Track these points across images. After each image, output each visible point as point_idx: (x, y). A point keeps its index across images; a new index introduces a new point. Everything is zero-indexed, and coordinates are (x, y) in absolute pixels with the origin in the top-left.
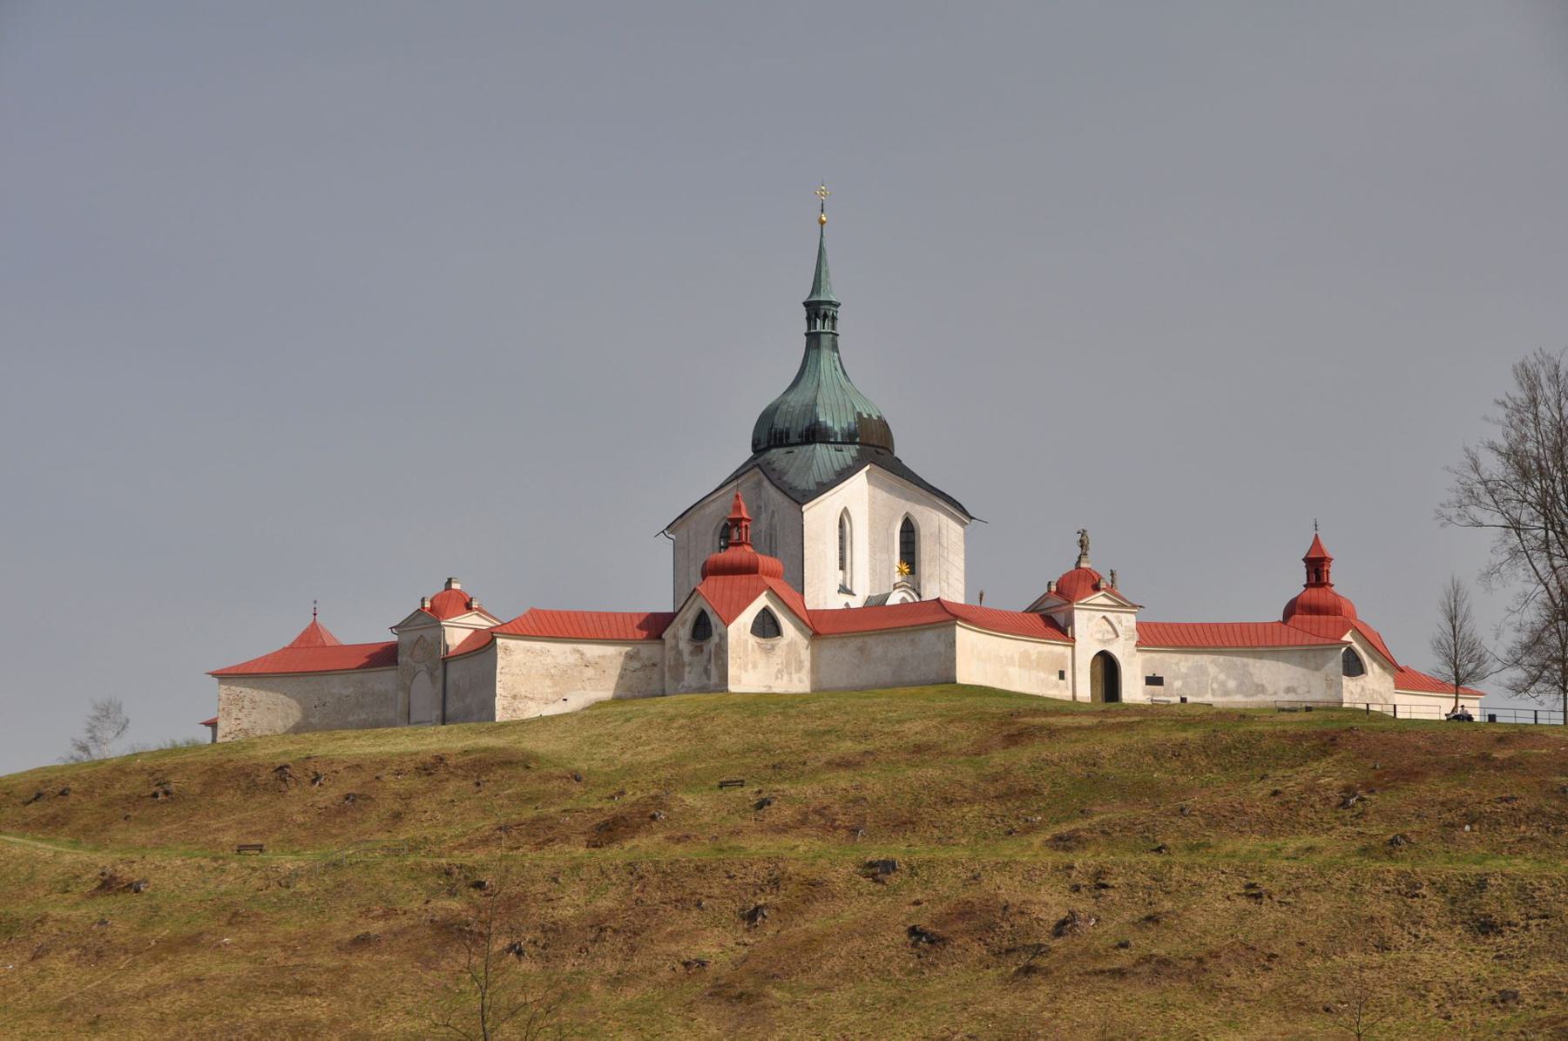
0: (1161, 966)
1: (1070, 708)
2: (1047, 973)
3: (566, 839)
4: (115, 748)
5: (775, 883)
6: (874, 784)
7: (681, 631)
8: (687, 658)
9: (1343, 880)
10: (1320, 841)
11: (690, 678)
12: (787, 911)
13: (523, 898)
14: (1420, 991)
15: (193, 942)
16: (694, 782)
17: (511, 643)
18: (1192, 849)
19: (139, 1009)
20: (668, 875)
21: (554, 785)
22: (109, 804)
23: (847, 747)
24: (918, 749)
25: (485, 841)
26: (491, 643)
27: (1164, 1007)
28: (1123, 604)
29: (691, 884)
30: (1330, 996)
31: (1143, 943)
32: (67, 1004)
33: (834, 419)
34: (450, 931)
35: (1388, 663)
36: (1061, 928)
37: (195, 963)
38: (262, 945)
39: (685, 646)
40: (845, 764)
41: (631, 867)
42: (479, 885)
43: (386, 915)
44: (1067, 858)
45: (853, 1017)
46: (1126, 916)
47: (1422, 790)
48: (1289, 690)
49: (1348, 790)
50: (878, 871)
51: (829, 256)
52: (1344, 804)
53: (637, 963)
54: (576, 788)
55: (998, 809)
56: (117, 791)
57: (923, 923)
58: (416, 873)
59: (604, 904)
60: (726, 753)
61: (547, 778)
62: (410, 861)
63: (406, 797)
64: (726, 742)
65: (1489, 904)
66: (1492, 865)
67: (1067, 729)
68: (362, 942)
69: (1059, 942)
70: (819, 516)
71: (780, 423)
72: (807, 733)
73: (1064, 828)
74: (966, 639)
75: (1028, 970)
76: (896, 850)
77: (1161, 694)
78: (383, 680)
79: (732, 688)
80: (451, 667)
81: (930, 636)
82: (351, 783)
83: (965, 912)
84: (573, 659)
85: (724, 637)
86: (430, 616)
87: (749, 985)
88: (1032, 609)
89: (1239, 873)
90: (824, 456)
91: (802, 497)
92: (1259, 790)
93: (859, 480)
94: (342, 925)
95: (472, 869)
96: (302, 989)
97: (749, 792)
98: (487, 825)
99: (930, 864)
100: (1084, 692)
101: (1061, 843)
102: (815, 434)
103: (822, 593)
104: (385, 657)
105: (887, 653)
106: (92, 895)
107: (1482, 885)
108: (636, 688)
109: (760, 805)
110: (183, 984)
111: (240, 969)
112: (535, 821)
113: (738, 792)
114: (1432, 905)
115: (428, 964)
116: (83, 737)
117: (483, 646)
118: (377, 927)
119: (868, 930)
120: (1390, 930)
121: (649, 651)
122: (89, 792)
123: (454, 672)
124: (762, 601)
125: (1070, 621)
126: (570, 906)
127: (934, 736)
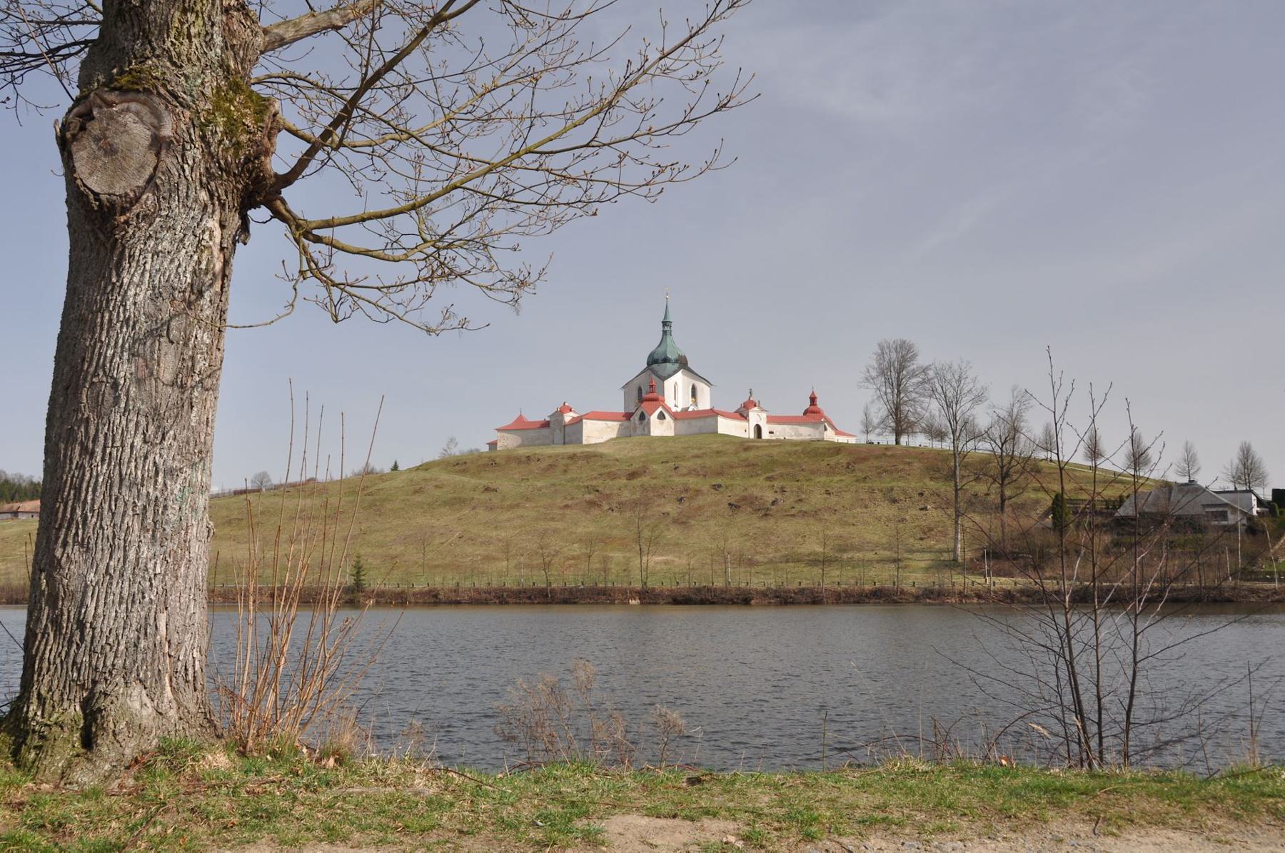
0: (804, 514)
1: (748, 440)
2: (771, 515)
3: (620, 478)
4: (456, 451)
5: (686, 491)
6: (708, 462)
7: (636, 418)
8: (638, 426)
9: (853, 488)
10: (843, 478)
11: (638, 432)
12: (691, 498)
13: (611, 494)
15: (517, 506)
17: (588, 421)
18: (807, 480)
19: (508, 524)
20: (654, 488)
21: (611, 463)
22: (479, 466)
23: (696, 452)
24: (718, 452)
25: (596, 478)
26: (581, 420)
27: (808, 525)
28: (762, 410)
29: (661, 491)
30: (853, 521)
31: (798, 507)
33: (671, 356)
34: (592, 504)
35: (833, 428)
36: (774, 503)
37: (520, 512)
38: (536, 507)
39: (637, 422)
40: (697, 456)
41: (642, 486)
42: (598, 491)
43: (572, 498)
44: (772, 483)
45: (717, 528)
46: (792, 499)
48: (809, 435)
49: (848, 464)
50: (716, 487)
51: (669, 309)
52: (848, 467)
53: (649, 513)
54: (617, 463)
56: (480, 463)
57: (732, 502)
58: (578, 487)
59: (635, 497)
60: (660, 453)
61: (609, 460)
63: (567, 465)
64: (659, 450)
65: (895, 495)
67: (761, 447)
68: (567, 506)
69: (772, 507)
70: (669, 384)
71: (656, 357)
72: (684, 448)
74: (720, 419)
75: (766, 515)
76: (718, 481)
77: (773, 437)
78: (545, 431)
79: (652, 434)
80: (567, 428)
81: (709, 420)
82: (550, 461)
83: (744, 498)
84: (605, 426)
85: (649, 420)
86: (560, 412)
87: (684, 519)
88: (736, 412)
89: (823, 487)
91: (664, 379)
93: (680, 373)
94: (560, 501)
95: (594, 486)
96: (553, 519)
97: (671, 464)
98: (595, 474)
99: (732, 485)
100: (752, 435)
101: (769, 479)
102: (666, 360)
104: (546, 425)
105: (697, 424)
106: (483, 492)
107: (892, 489)
108: (624, 434)
109: (676, 468)
110: (518, 517)
111: (533, 514)
112: (609, 473)
113: (668, 465)
114: (879, 495)
115: (587, 513)
117: (578, 422)
118: (570, 502)
121: (626, 423)
122: (472, 463)
123: (567, 429)
124: (660, 409)
125: (748, 415)
126: (626, 496)
127: (721, 449)
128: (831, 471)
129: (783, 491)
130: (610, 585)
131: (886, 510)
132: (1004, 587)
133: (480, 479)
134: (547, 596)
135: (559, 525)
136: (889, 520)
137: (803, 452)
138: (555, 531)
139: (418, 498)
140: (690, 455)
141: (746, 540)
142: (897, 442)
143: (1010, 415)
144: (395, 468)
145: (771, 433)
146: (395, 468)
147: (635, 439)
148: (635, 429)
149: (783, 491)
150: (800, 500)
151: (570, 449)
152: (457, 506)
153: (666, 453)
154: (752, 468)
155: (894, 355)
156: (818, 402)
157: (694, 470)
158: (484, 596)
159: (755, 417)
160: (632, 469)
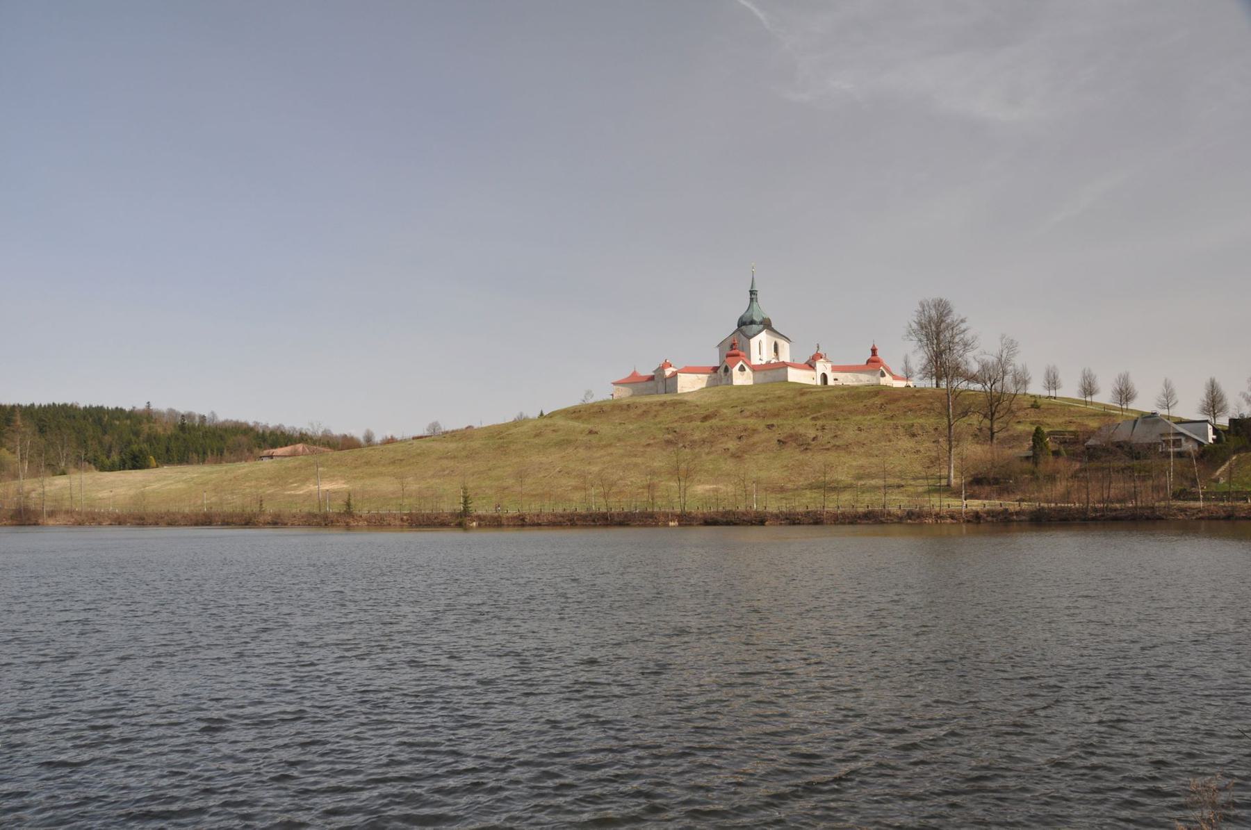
1: (816, 386)
2: (810, 449)
4: (591, 401)
6: (769, 406)
7: (722, 370)
9: (880, 426)
11: (724, 382)
12: (749, 436)
14: (898, 451)
15: (610, 445)
16: (725, 407)
18: (845, 419)
19: (599, 460)
20: (720, 429)
24: (779, 397)
27: (838, 457)
30: (877, 453)
31: (834, 442)
32: (583, 459)
33: (757, 319)
34: (669, 442)
35: (891, 374)
36: (814, 439)
37: (610, 450)
39: (722, 374)
41: (711, 427)
43: (654, 439)
47: (899, 404)
49: (882, 404)
50: (770, 427)
52: (881, 408)
53: (713, 449)
55: (798, 411)
57: (781, 438)
58: (660, 429)
59: (705, 435)
62: (659, 426)
63: (657, 411)
64: (733, 397)
66: (915, 421)
68: (649, 445)
70: (754, 342)
71: (744, 320)
73: (815, 415)
74: (790, 370)
75: (806, 449)
76: (774, 422)
77: (839, 383)
78: (651, 384)
79: (734, 384)
81: (781, 370)
82: (644, 408)
83: (791, 436)
86: (662, 369)
87: (740, 454)
90: (754, 327)
91: (750, 338)
92: (861, 405)
94: (644, 441)
97: (739, 409)
98: (677, 418)
99: (782, 425)
100: (819, 383)
101: (814, 419)
102: (752, 322)
103: (755, 360)
104: (652, 378)
105: (771, 375)
108: (712, 384)
109: (742, 411)
110: (608, 455)
111: (621, 451)
112: (688, 416)
113: (736, 409)
114: (901, 431)
115: (664, 450)
116: (583, 398)
117: (674, 375)
118: (652, 442)
119: (768, 441)
120: (892, 437)
121: (714, 375)
122: (586, 411)
123: (668, 381)
124: (741, 363)
128: (867, 410)
129: (823, 428)
130: (656, 509)
131: (906, 443)
132: (974, 508)
133: (589, 423)
134: (607, 519)
135: (639, 460)
136: (907, 451)
137: (848, 396)
138: (636, 465)
139: (537, 441)
140: (758, 399)
141: (785, 471)
142: (937, 385)
143: (1000, 360)
144: (542, 414)
145: (836, 380)
146: (542, 414)
147: (718, 388)
148: (721, 380)
149: (823, 428)
150: (836, 436)
151: (667, 398)
152: (565, 446)
153: (739, 398)
154: (802, 409)
155: (933, 313)
156: (879, 353)
157: (756, 413)
158: (560, 519)
159: (821, 366)
160: (706, 413)
